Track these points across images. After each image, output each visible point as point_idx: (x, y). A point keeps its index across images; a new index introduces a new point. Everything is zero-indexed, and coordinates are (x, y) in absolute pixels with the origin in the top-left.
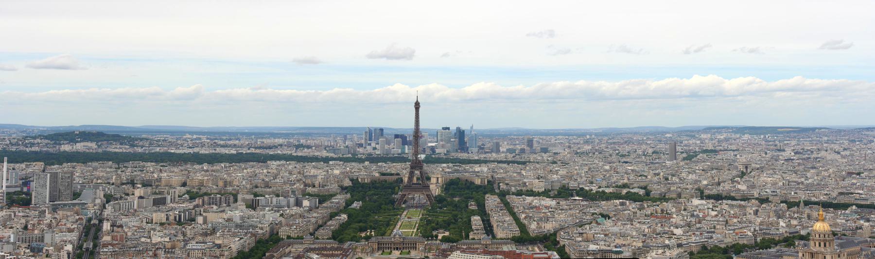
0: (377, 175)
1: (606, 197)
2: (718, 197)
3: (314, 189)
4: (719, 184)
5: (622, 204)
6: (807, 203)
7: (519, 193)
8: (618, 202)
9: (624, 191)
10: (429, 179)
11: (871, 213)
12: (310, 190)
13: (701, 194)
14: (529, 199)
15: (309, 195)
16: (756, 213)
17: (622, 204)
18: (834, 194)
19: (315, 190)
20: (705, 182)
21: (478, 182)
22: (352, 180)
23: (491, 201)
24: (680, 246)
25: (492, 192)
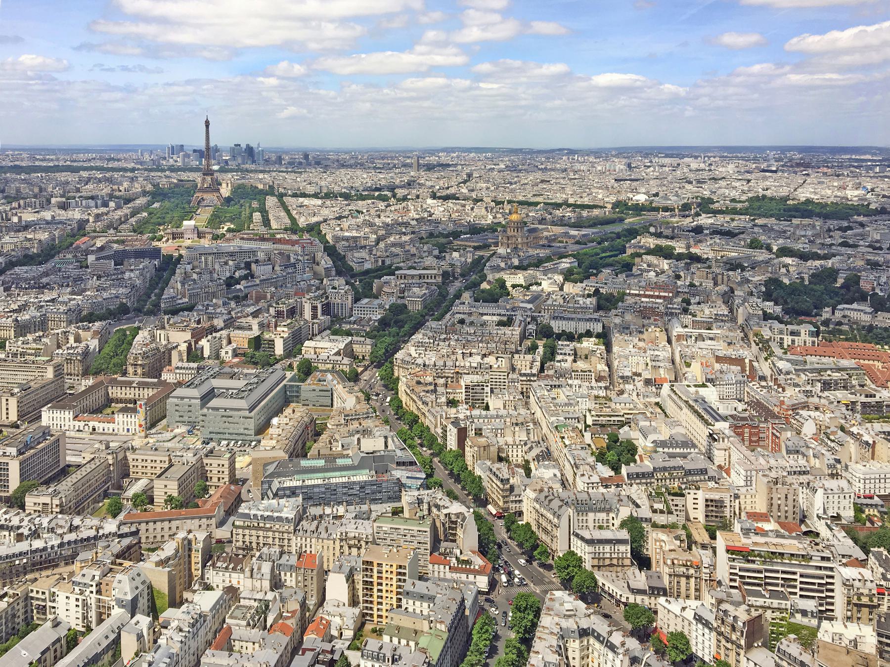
0: (175, 181)
1: (363, 198)
2: (446, 198)
3: (120, 193)
4: (448, 188)
5: (373, 203)
6: (509, 202)
7: (295, 195)
8: (370, 201)
9: (377, 194)
10: (221, 184)
11: (553, 209)
12: (117, 193)
13: (434, 196)
14: (301, 200)
15: (117, 198)
16: (472, 209)
17: (373, 203)
18: (529, 196)
19: (120, 193)
20: (438, 187)
21: (261, 187)
22: (154, 186)
23: (271, 202)
24: (413, 233)
25: (273, 194)
